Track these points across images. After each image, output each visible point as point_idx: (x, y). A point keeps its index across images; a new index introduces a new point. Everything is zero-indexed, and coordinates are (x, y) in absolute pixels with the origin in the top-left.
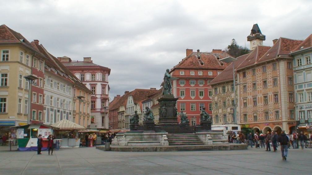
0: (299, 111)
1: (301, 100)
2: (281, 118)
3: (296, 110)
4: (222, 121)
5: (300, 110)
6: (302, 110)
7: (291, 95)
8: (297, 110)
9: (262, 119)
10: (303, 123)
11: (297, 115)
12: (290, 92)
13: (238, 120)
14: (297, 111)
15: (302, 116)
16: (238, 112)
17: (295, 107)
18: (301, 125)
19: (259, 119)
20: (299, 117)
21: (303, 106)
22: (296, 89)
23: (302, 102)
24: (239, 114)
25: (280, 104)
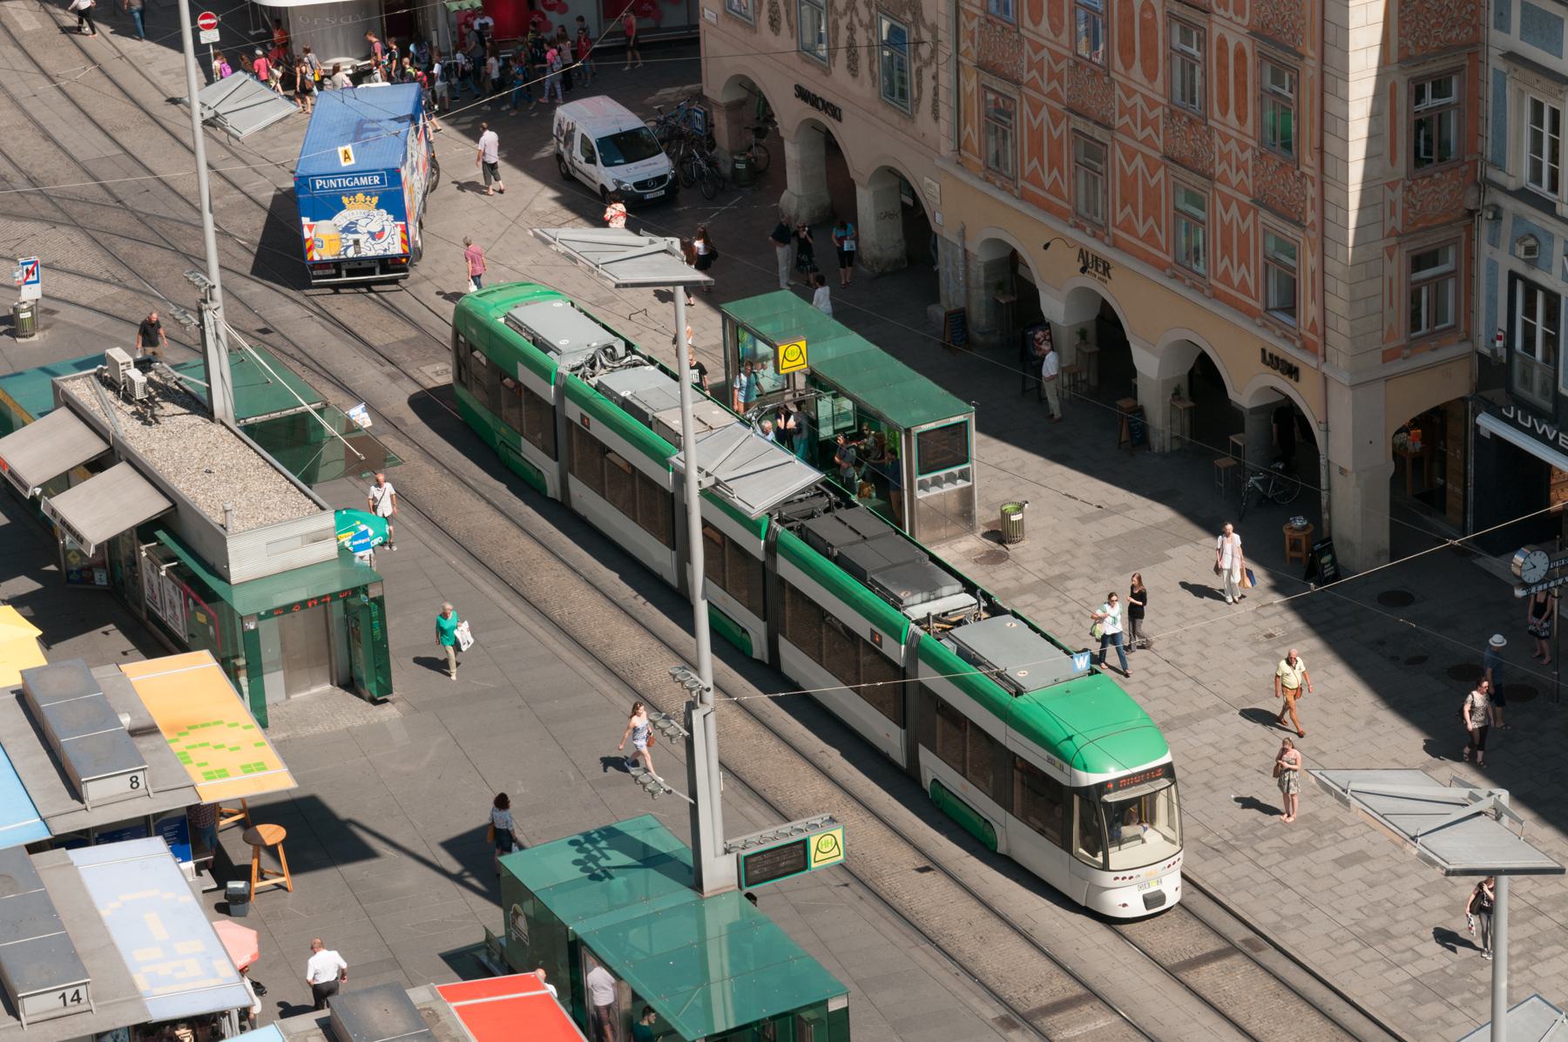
0: (1513, 277)
1: (1536, 167)
2: (1313, 328)
3: (1485, 250)
4: (784, 24)
5: (1520, 268)
6: (1538, 276)
7: (1441, 89)
8: (1498, 258)
9: (1150, 238)
10: (1539, 414)
11: (1492, 300)
12: (1419, 71)
13: (936, 118)
14: (1493, 266)
15: (1529, 331)
16: (934, 29)
17: (1471, 213)
18: (1513, 423)
19: (1128, 227)
20: (1502, 324)
21: (1550, 237)
22: (1503, 24)
23: (1544, 189)
24: (947, 49)
25: (1312, 192)
